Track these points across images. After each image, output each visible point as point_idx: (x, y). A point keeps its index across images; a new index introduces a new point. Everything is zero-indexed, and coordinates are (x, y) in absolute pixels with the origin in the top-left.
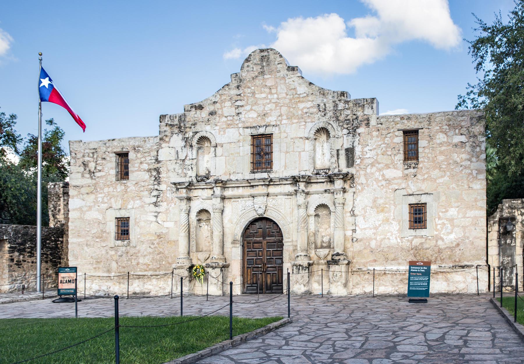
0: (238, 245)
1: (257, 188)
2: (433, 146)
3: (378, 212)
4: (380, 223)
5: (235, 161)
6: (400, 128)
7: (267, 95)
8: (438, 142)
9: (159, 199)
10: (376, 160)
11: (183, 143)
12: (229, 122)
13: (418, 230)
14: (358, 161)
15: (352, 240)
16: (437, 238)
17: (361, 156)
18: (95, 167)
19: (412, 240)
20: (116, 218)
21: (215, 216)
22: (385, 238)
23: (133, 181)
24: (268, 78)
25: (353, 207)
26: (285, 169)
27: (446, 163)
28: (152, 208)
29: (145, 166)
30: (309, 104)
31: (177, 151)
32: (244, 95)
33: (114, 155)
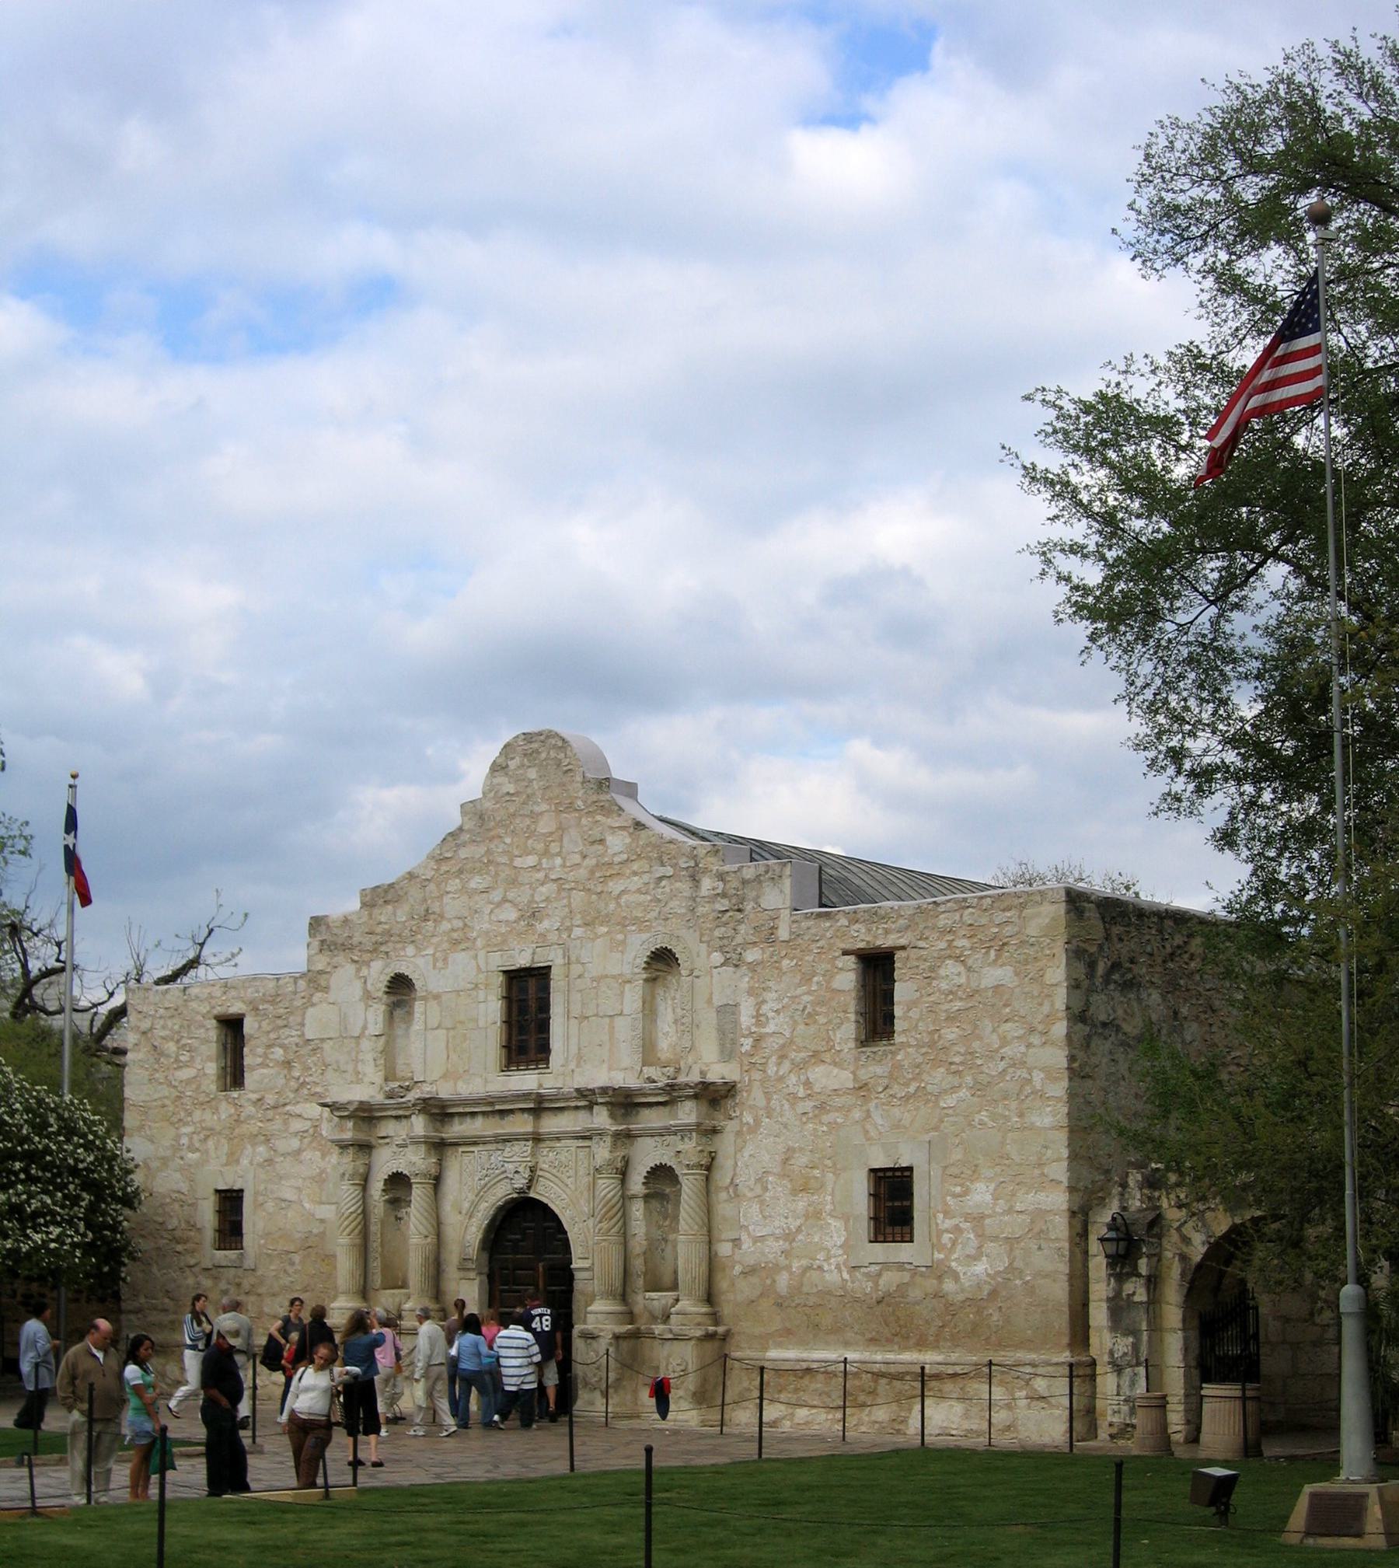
1: (511, 1118)
2: (931, 999)
3: (794, 1192)
4: (798, 1223)
6: (848, 946)
7: (540, 860)
8: (944, 986)
9: (306, 1141)
10: (792, 1042)
11: (358, 992)
12: (455, 935)
14: (747, 1044)
16: (938, 1271)
17: (754, 1029)
18: (177, 1056)
19: (879, 1275)
20: (217, 1191)
21: (419, 1194)
22: (810, 1268)
23: (252, 1092)
24: (541, 813)
25: (734, 1175)
26: (578, 1065)
27: (962, 1051)
29: (278, 1053)
30: (637, 882)
32: (489, 861)
33: (214, 1021)
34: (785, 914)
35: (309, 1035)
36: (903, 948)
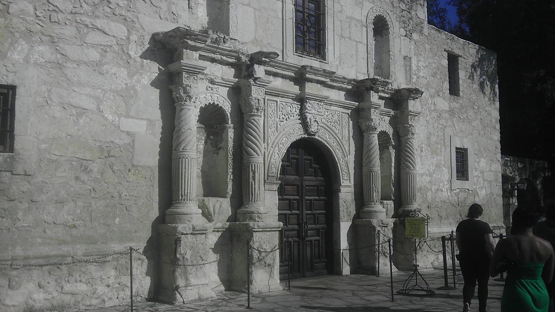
0: (276, 187)
5: (270, 24)
22: (438, 190)
34: (426, 22)
36: (461, 56)
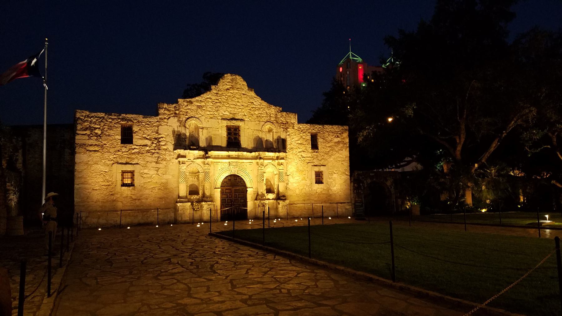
9: (159, 159)
11: (179, 124)
13: (320, 184)
15: (287, 188)
28: (154, 164)
31: (174, 128)
35: (159, 132)
